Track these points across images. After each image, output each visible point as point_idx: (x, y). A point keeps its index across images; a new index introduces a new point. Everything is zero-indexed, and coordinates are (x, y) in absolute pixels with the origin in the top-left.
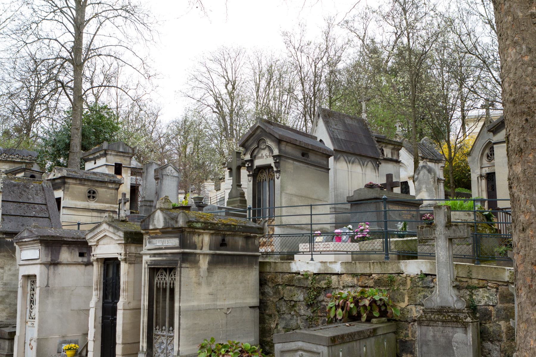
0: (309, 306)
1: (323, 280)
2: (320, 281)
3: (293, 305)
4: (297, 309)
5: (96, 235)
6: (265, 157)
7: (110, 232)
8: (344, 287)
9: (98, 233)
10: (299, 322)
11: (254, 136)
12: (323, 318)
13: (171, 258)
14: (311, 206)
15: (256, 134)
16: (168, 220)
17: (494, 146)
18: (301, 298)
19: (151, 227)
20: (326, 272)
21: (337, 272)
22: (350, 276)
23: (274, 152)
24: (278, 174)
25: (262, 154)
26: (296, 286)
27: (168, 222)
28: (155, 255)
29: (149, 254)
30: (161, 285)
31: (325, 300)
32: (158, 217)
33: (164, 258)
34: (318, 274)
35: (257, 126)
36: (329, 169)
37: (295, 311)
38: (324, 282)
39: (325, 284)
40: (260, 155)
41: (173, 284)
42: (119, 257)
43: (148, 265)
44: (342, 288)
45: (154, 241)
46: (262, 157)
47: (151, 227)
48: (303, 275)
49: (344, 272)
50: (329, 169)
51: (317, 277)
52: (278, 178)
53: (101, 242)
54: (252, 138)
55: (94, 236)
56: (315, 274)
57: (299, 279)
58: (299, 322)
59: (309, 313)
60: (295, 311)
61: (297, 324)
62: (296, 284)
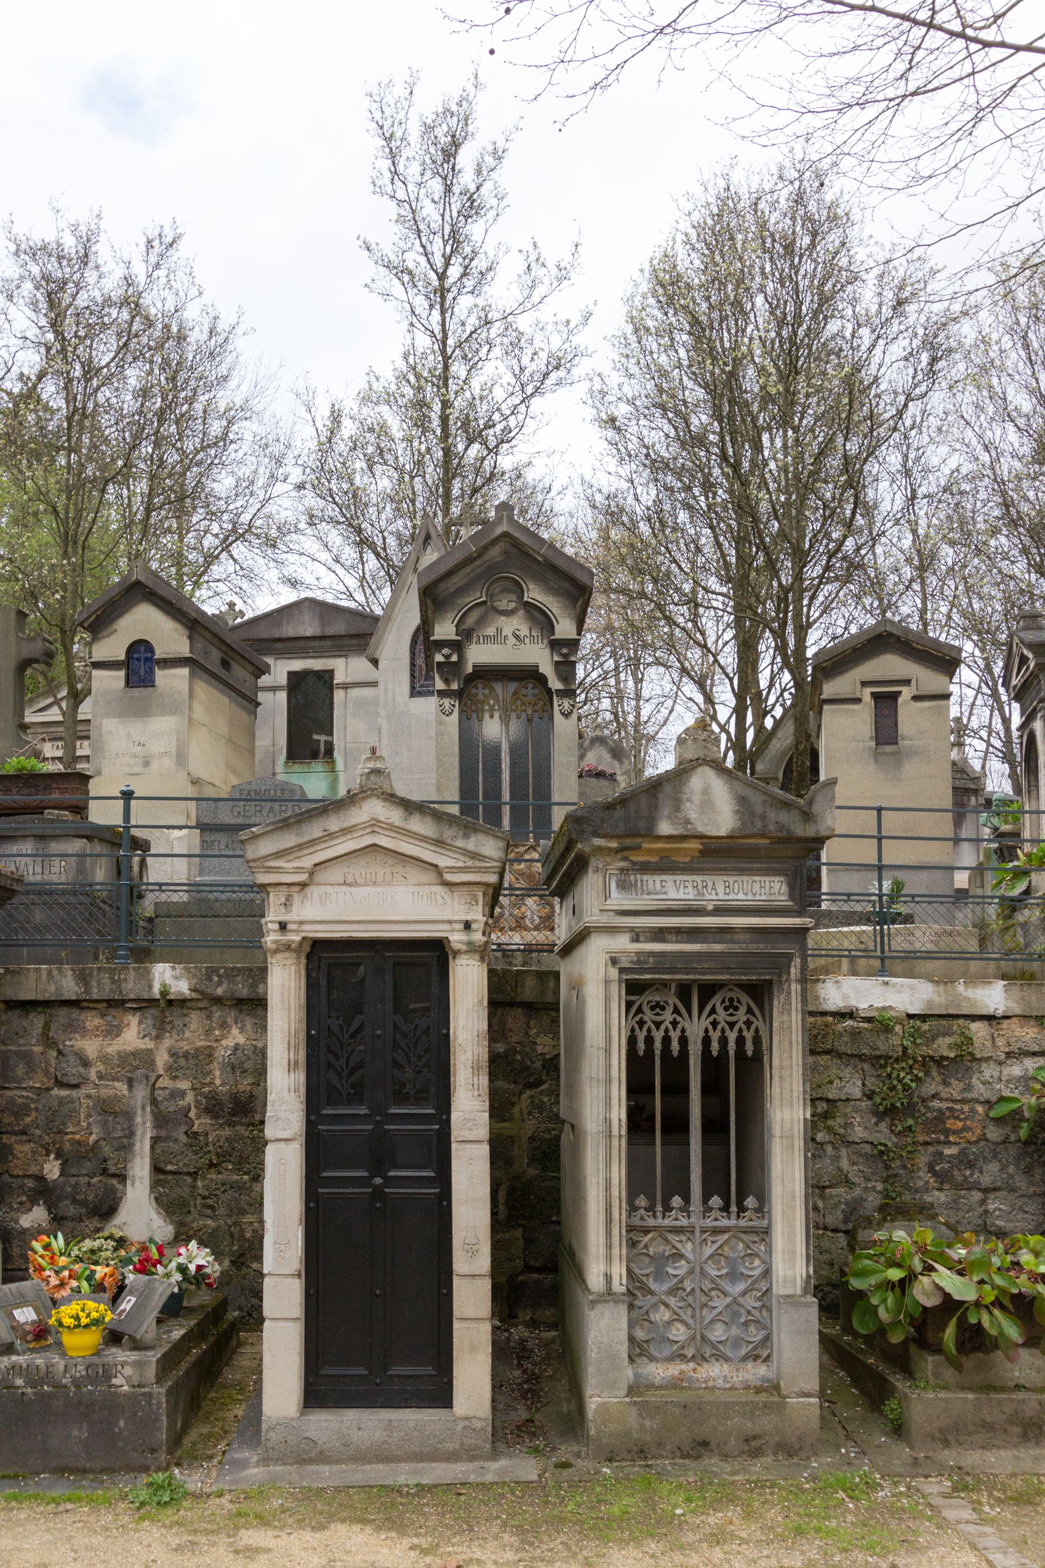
0: (887, 1113)
1: (944, 1035)
2: (934, 1039)
3: (826, 1112)
4: (836, 1123)
5: (313, 842)
6: (512, 640)
7: (425, 839)
8: (1008, 1055)
9: (331, 836)
10: (845, 1164)
11: (477, 563)
12: (931, 1149)
13: (756, 948)
14: (879, 810)
15: (486, 557)
16: (759, 809)
17: (825, 707)
18: (855, 1089)
19: (665, 828)
20: (951, 1012)
21: (990, 1011)
22: (1032, 1023)
23: (558, 628)
24: (566, 704)
25: (499, 630)
26: (840, 1056)
27: (763, 817)
28: (660, 934)
29: (631, 929)
30: (658, 1045)
31: (944, 1095)
32: (706, 791)
33: (717, 947)
34: (923, 1017)
35: (499, 531)
36: (259, 704)
37: (830, 1129)
38: (948, 1040)
39: (950, 1047)
40: (490, 631)
41: (757, 1040)
42: (457, 938)
43: (622, 971)
44: (1003, 1057)
45: (653, 881)
46: (499, 638)
47: (665, 828)
48: (869, 1020)
49: (1018, 1012)
50: (259, 704)
51: (926, 1027)
52: (567, 715)
53: (319, 877)
54: (468, 569)
55: (300, 847)
56: (911, 1016)
57: (855, 1034)
58: (845, 1164)
59: (883, 1134)
60: (830, 1129)
61: (839, 1169)
62: (843, 1049)
